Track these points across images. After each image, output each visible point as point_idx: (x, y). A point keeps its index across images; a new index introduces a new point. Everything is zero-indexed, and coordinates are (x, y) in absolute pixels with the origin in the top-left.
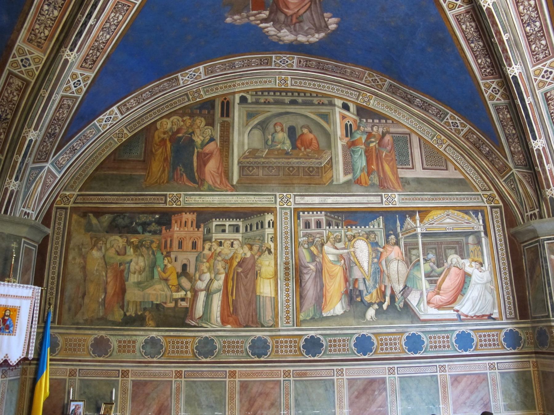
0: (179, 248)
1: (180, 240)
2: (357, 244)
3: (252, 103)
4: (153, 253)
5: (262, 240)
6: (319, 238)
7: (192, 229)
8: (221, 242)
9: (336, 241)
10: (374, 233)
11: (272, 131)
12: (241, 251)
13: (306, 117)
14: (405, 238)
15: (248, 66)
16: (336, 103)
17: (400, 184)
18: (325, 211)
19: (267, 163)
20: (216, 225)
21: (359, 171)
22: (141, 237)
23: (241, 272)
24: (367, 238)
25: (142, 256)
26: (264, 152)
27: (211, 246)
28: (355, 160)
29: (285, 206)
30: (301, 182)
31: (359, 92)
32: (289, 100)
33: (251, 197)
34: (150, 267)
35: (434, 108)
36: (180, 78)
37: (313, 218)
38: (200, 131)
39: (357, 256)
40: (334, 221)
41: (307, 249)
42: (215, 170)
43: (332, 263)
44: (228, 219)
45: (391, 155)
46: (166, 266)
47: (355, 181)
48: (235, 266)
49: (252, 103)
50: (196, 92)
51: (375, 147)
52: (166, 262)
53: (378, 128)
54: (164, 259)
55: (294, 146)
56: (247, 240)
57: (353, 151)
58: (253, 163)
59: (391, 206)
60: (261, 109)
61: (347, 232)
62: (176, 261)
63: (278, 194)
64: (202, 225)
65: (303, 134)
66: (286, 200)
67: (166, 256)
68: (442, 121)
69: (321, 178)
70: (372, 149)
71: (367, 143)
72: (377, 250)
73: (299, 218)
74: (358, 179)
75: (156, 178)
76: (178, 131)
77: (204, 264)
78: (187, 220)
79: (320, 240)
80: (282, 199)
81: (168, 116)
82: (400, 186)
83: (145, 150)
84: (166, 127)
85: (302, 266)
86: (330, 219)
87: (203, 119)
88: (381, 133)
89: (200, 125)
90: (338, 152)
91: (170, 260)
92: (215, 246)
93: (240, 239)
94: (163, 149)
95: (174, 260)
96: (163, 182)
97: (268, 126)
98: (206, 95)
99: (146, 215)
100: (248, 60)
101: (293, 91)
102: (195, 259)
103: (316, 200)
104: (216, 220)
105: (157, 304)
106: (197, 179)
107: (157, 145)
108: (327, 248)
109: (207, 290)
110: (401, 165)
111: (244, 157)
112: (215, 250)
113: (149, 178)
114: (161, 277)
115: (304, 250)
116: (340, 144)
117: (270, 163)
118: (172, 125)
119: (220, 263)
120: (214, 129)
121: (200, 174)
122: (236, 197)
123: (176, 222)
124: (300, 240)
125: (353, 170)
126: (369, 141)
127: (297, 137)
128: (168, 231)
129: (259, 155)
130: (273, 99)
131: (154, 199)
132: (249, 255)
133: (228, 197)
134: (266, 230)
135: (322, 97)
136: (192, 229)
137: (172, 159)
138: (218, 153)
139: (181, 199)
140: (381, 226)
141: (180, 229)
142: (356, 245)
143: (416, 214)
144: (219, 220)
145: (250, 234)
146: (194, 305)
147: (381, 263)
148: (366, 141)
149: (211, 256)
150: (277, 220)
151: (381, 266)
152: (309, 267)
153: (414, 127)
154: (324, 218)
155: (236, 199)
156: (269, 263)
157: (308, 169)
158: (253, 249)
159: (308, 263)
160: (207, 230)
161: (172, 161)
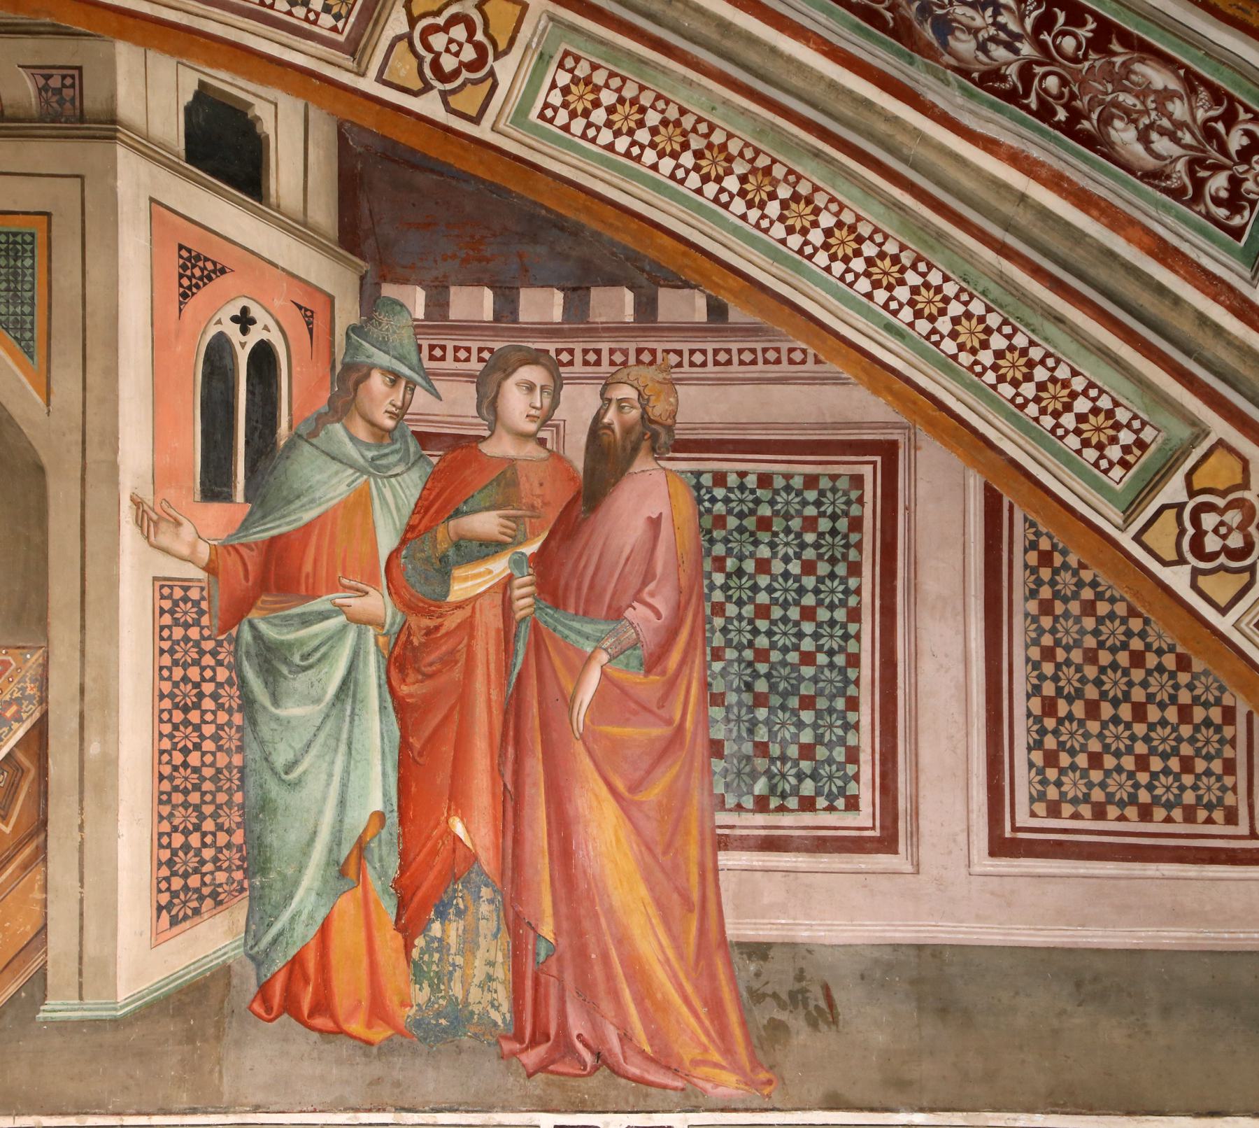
16: (128, 106)
17: (733, 1017)
21: (311, 877)
28: (281, 758)
45: (664, 700)
47: (264, 991)
51: (507, 606)
53: (558, 383)
70: (468, 626)
74: (296, 963)
82: (723, 1032)
88: (576, 454)
110: (761, 805)
126: (446, 532)
148: (410, 534)
153: (948, 365)
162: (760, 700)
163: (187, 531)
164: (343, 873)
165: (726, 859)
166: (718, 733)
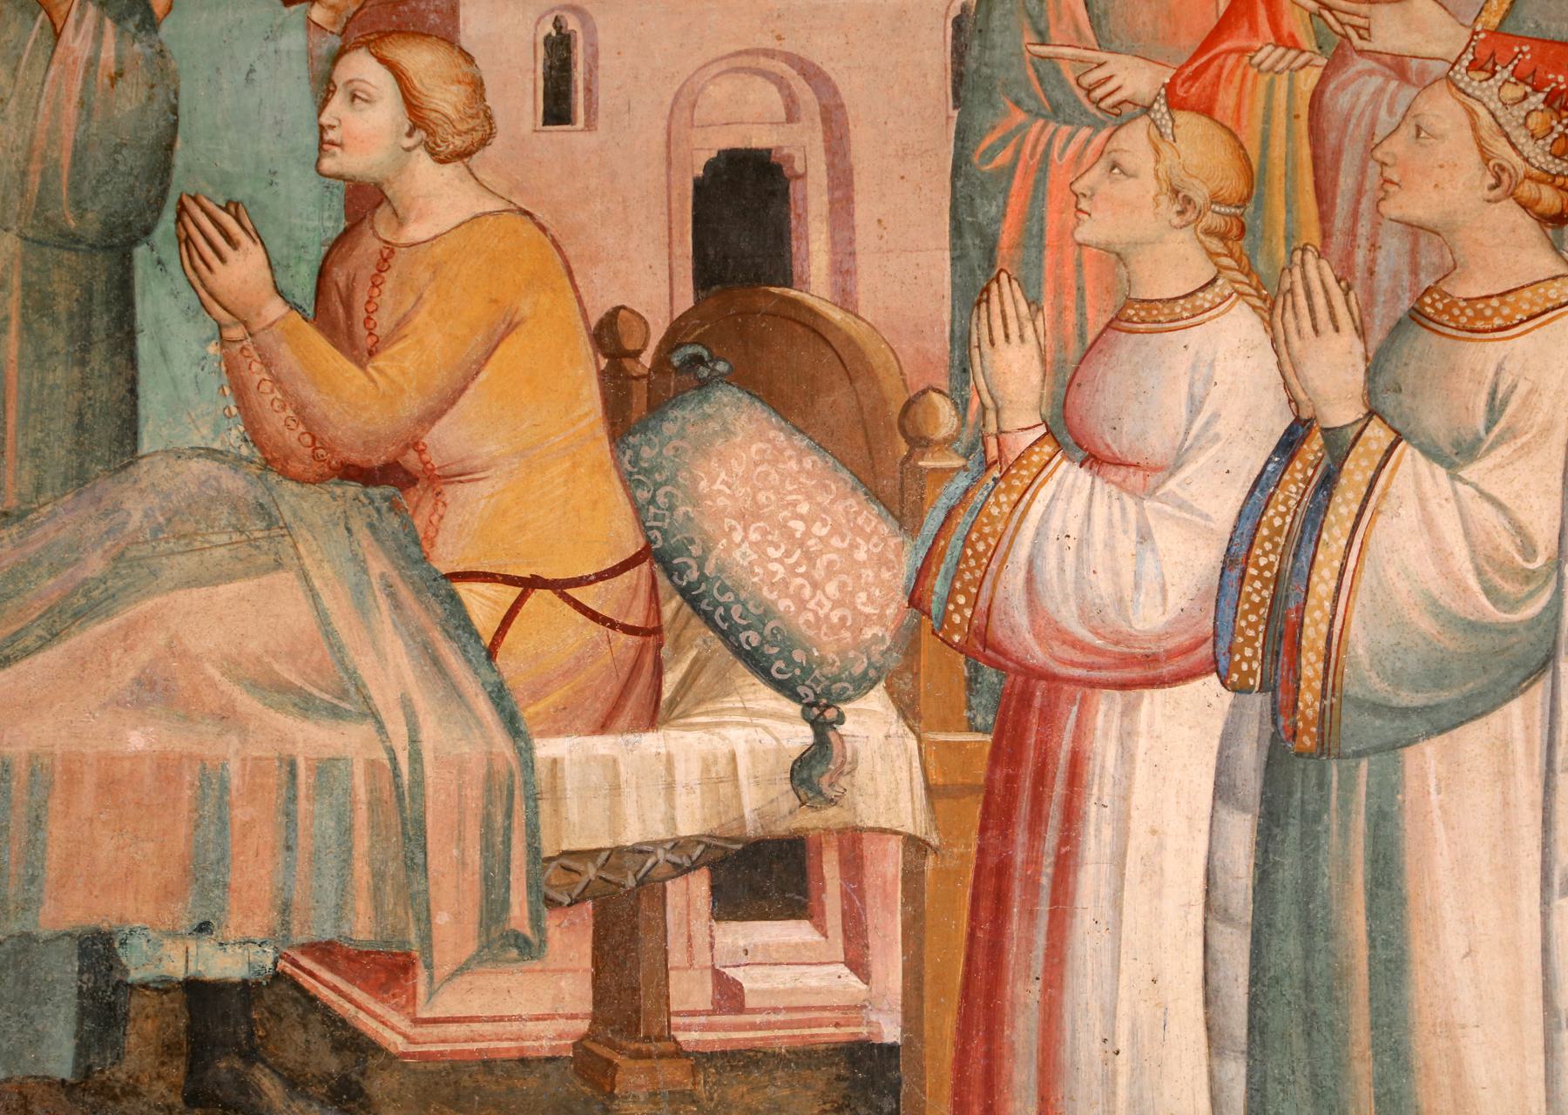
102: (935, 55)
105: (197, 991)
109: (1250, 659)
114: (278, 422)
119: (1442, 110)
146: (1024, 994)
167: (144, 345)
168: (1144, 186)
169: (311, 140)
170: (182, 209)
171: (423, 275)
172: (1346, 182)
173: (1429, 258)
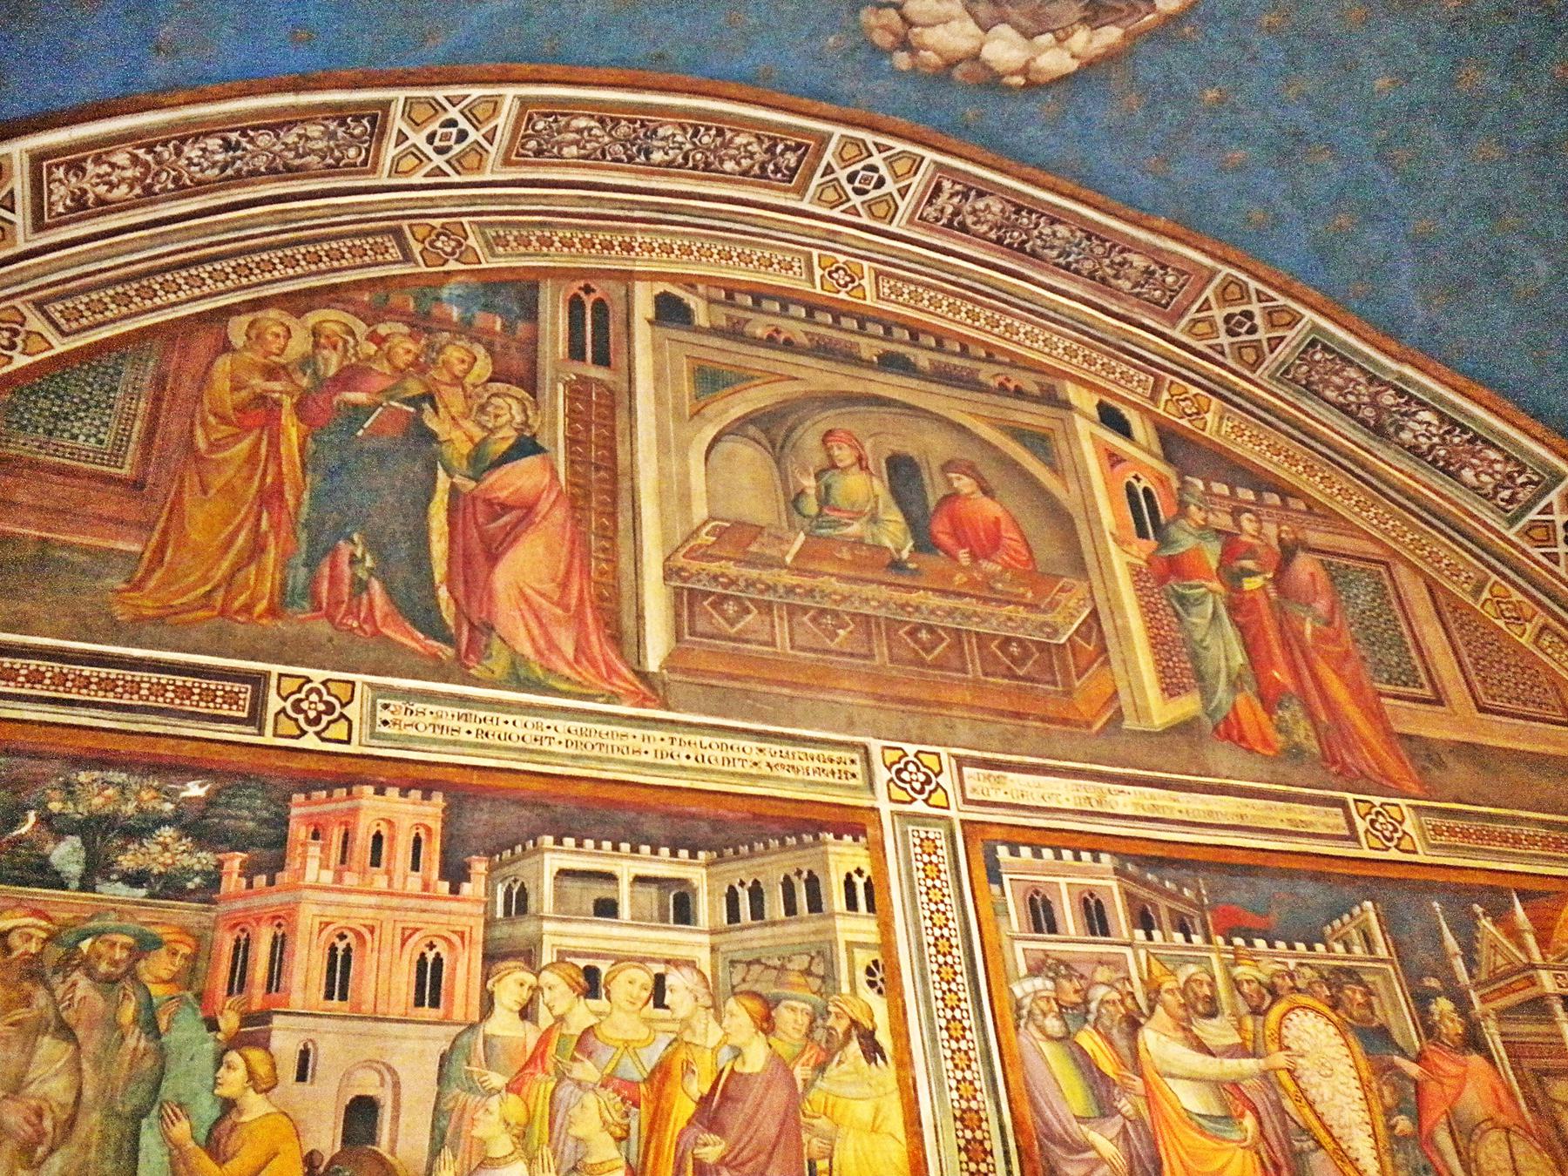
0: (329, 996)
1: (341, 946)
2: (1294, 1031)
3: (714, 331)
4: (150, 1024)
5: (823, 978)
6: (1110, 985)
7: (414, 883)
8: (591, 973)
9: (1194, 1008)
10: (1360, 982)
11: (818, 459)
12: (715, 1035)
13: (961, 429)
14: (1503, 1015)
15: (707, 167)
18: (1114, 854)
19: (810, 593)
20: (564, 873)
22: (66, 904)
23: (722, 1161)
24: (1335, 1005)
25: (65, 1031)
26: (790, 542)
27: (536, 989)
28: (1197, 637)
29: (919, 807)
30: (977, 703)
31: (1157, 378)
32: (875, 351)
33: (743, 743)
34: (111, 1113)
35: (1493, 455)
36: (397, 123)
37: (1062, 881)
38: (467, 397)
39: (1313, 1094)
40: (1163, 904)
41: (1059, 1040)
42: (549, 587)
43: (1201, 1130)
44: (625, 847)
46: (229, 1105)
47: (1216, 728)
48: (682, 1124)
49: (714, 331)
50: (445, 232)
52: (233, 1080)
54: (219, 1062)
55: (925, 543)
56: (740, 968)
57: (1182, 599)
58: (742, 583)
59: (1394, 855)
60: (760, 365)
61: (1236, 964)
62: (301, 1077)
63: (875, 746)
64: (479, 866)
65: (952, 497)
66: (922, 778)
67: (237, 1042)
68: (1512, 522)
69: (1068, 693)
71: (1231, 576)
72: (1393, 1067)
73: (994, 876)
75: (205, 579)
76: (349, 377)
77: (494, 1102)
78: (385, 833)
79: (1115, 996)
80: (899, 771)
81: (298, 303)
83: (150, 433)
84: (282, 350)
85: (1051, 1136)
86: (1143, 893)
87: (480, 351)
89: (467, 372)
90: (1117, 593)
91: (262, 1070)
92: (558, 994)
93: (704, 959)
94: (260, 439)
95: (289, 1070)
96: (248, 608)
97: (795, 435)
98: (494, 255)
99: (118, 777)
100: (720, 132)
101: (889, 325)
103: (1064, 792)
104: (558, 842)
106: (448, 612)
107: (223, 419)
108: (1159, 1041)
110: (1388, 682)
111: (691, 549)
112: (560, 1019)
113: (158, 574)
115: (1047, 1048)
116: (1119, 562)
117: (824, 595)
118: (316, 345)
119: (590, 1099)
120: (537, 406)
121: (468, 597)
122: (666, 735)
123: (316, 836)
124: (1018, 993)
125: (1200, 676)
127: (932, 501)
128: (261, 880)
129: (768, 551)
130: (807, 333)
131: (186, 692)
132: (756, 1059)
133: (621, 730)
134: (840, 923)
135: (1012, 365)
136: (414, 883)
137: (306, 496)
138: (559, 514)
139: (352, 711)
140: (1382, 951)
141: (339, 878)
142: (1290, 1035)
143: (1511, 903)
144: (579, 845)
145: (755, 938)
147: (1431, 1139)
149: (536, 1058)
150: (886, 875)
151: (1436, 1158)
152: (1091, 1147)
154: (1113, 884)
155: (666, 746)
156: (877, 1110)
157: (1000, 647)
158: (778, 1022)
159: (1081, 1120)
160: (509, 889)
161: (305, 509)
162: (1373, 644)
163: (1135, 547)
164: (1234, 685)
165: (1383, 700)
166: (1363, 653)
167: (141, 1155)
168: (495, 1118)
169: (211, 1082)
170: (162, 1106)
171: (245, 1134)
172: (559, 1120)
173: (581, 1149)
